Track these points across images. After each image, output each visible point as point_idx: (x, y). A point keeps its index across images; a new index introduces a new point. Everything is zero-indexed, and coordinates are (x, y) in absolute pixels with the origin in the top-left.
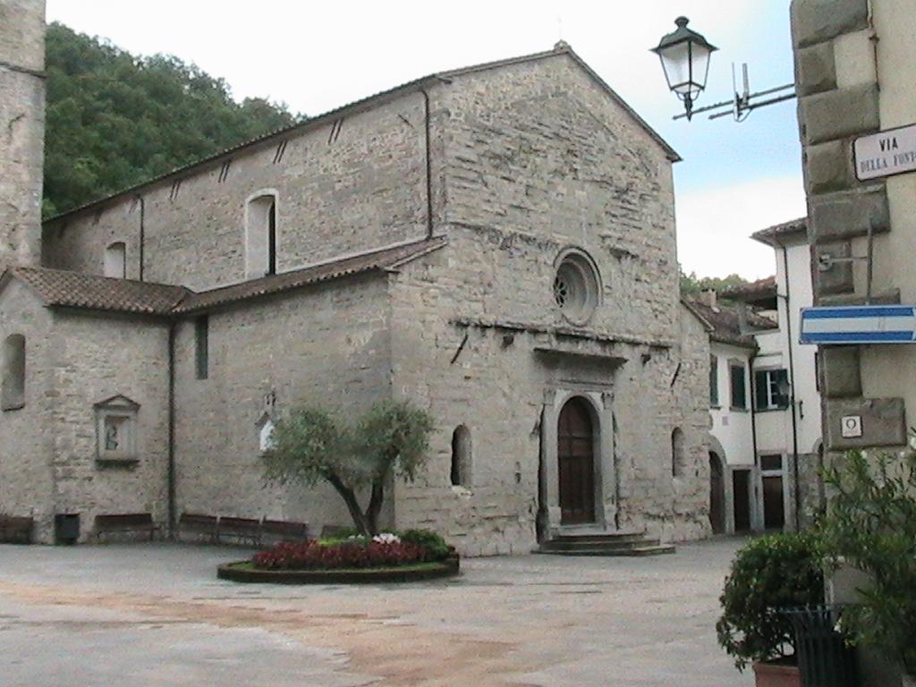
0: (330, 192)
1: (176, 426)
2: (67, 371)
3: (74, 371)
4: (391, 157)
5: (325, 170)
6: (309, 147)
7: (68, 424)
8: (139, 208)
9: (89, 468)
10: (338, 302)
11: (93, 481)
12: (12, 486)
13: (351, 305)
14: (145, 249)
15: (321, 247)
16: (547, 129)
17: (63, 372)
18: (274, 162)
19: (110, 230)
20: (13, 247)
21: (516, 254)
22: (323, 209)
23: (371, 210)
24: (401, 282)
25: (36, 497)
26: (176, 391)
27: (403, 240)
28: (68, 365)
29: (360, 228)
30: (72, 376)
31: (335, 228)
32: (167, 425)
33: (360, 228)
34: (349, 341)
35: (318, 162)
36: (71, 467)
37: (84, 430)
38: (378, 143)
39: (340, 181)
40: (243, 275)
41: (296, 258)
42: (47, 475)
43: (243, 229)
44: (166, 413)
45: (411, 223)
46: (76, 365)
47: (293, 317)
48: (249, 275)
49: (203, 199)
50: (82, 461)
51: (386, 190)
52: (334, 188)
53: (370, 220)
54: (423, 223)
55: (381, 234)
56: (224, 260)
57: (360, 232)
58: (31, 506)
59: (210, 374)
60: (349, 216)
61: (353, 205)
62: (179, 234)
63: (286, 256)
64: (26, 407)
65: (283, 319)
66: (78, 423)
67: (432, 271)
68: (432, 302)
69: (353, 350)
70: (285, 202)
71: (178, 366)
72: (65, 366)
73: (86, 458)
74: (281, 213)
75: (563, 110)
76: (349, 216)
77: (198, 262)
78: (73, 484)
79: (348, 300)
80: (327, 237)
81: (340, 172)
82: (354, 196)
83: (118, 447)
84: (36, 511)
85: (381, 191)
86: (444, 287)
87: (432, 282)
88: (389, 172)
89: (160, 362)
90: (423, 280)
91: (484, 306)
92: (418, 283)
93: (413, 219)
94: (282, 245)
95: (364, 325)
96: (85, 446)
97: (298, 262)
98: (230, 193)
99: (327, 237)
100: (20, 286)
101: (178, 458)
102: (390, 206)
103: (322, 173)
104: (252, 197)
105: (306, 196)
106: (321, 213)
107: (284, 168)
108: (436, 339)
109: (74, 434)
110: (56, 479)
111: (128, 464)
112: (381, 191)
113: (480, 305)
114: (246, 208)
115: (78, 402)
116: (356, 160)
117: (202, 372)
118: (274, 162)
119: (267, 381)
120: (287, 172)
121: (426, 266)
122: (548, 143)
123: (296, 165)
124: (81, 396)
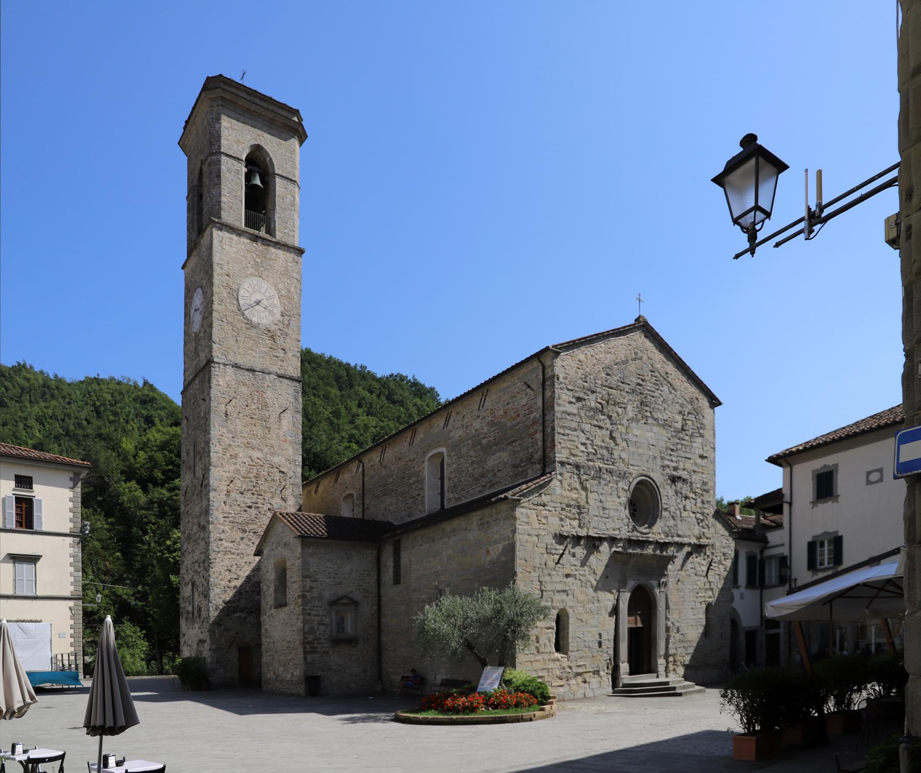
0: (479, 446)
1: (382, 616)
2: (311, 581)
3: (316, 581)
7: (312, 617)
8: (361, 469)
9: (326, 645)
10: (481, 525)
11: (330, 654)
12: (281, 658)
15: (474, 487)
16: (627, 386)
17: (309, 582)
18: (444, 428)
19: (345, 486)
20: (283, 499)
22: (473, 459)
23: (504, 455)
25: (294, 665)
26: (382, 593)
27: (526, 477)
28: (311, 577)
29: (499, 471)
30: (314, 585)
31: (482, 472)
32: (376, 615)
33: (499, 471)
34: (488, 552)
35: (471, 425)
36: (315, 645)
37: (323, 621)
39: (486, 437)
40: (425, 511)
41: (457, 496)
42: (301, 650)
43: (424, 479)
44: (375, 607)
45: (531, 463)
46: (317, 577)
47: (453, 538)
48: (428, 511)
49: (400, 459)
50: (322, 641)
52: (481, 444)
53: (505, 464)
54: (539, 463)
55: (511, 474)
57: (498, 474)
58: (291, 671)
59: (402, 581)
60: (492, 462)
61: (494, 454)
63: (451, 496)
64: (286, 608)
65: (446, 540)
66: (318, 615)
67: (545, 498)
68: (544, 521)
69: (491, 558)
70: (450, 456)
71: (382, 576)
72: (309, 577)
73: (325, 639)
74: (449, 465)
75: (639, 372)
76: (492, 462)
77: (397, 503)
78: (316, 656)
79: (487, 522)
80: (477, 480)
81: (485, 430)
82: (495, 448)
83: (345, 631)
84: (295, 673)
85: (513, 442)
86: (553, 509)
87: (544, 506)
88: (518, 427)
89: (371, 573)
90: (538, 505)
92: (534, 507)
93: (533, 460)
95: (497, 542)
96: (324, 631)
97: (459, 498)
98: (416, 453)
99: (477, 480)
100: (282, 524)
101: (384, 638)
103: (473, 432)
104: (430, 455)
105: (464, 451)
106: (473, 462)
109: (316, 623)
110: (305, 653)
111: (352, 641)
112: (513, 442)
114: (426, 464)
115: (319, 602)
116: (496, 421)
117: (397, 580)
118: (444, 428)
119: (436, 583)
120: (452, 434)
121: (540, 495)
122: (630, 397)
123: (457, 428)
124: (320, 598)
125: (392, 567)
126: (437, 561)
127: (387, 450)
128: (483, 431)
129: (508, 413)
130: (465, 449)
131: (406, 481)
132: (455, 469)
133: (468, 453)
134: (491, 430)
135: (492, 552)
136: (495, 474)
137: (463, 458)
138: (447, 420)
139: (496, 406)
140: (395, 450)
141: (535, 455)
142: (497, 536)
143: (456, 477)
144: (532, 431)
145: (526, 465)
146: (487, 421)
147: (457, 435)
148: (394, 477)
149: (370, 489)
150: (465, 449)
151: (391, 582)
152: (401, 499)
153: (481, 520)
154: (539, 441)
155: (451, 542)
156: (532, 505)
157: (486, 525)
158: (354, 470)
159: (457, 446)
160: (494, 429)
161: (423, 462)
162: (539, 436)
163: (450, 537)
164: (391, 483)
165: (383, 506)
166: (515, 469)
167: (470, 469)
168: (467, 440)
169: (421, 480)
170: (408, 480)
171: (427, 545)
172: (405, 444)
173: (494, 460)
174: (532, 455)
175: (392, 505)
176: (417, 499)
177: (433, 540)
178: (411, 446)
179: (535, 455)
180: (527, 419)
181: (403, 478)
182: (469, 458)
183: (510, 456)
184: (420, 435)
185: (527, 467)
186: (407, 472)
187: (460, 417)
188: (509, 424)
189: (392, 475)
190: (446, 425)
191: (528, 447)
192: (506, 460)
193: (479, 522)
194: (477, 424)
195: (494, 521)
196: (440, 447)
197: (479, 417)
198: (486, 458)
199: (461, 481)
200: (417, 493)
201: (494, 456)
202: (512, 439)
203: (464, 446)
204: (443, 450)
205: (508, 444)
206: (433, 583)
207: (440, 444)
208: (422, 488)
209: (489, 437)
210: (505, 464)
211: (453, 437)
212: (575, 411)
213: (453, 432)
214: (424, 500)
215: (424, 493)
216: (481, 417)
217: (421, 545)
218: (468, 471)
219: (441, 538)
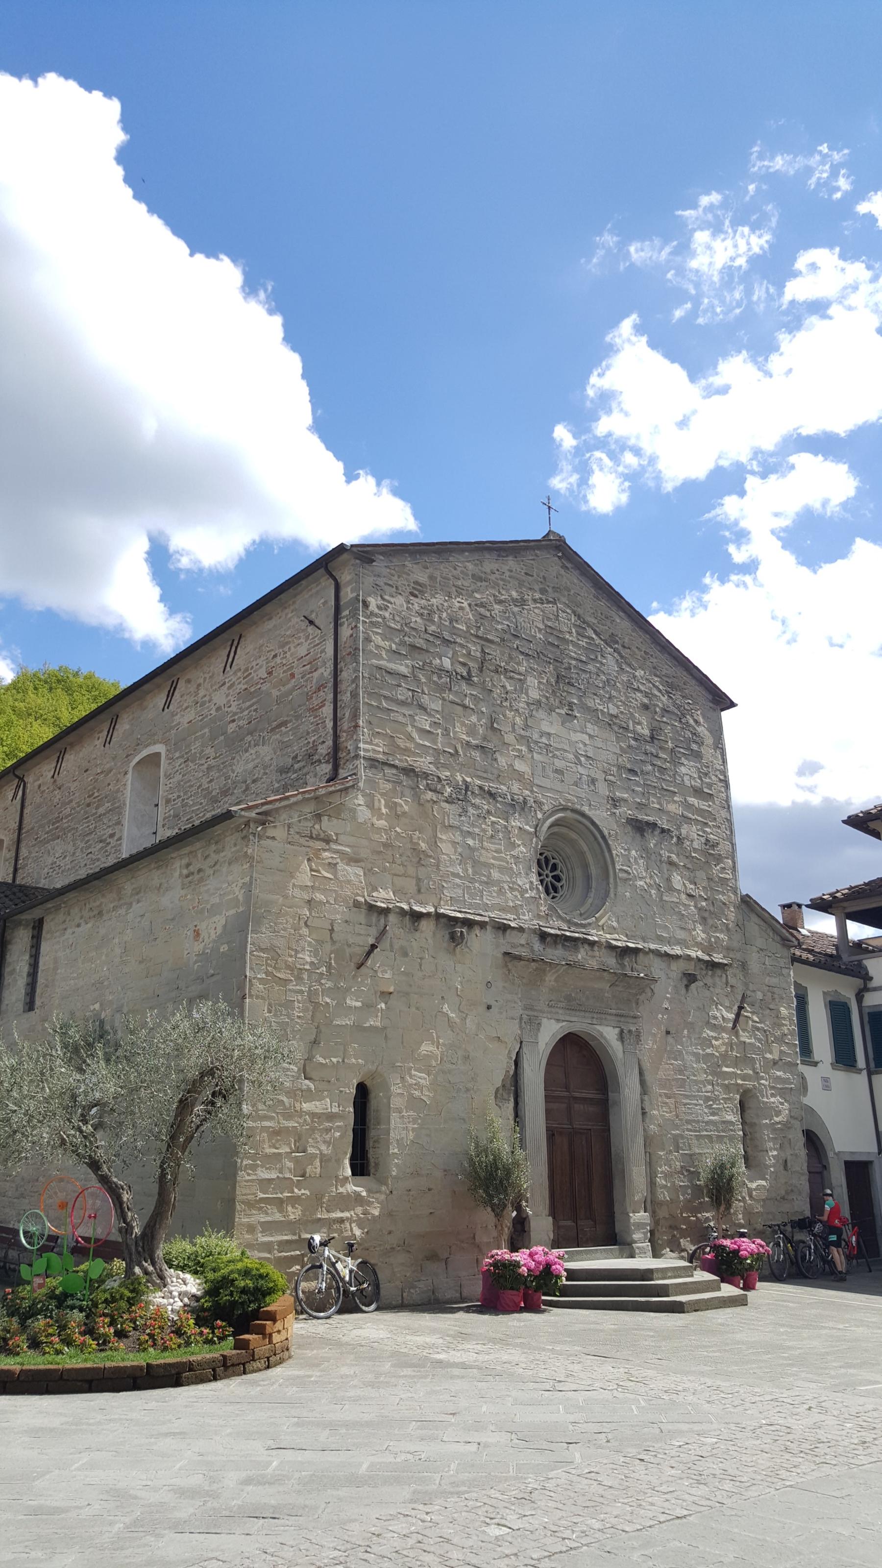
0: (222, 738)
4: (293, 676)
5: (219, 709)
6: (201, 681)
10: (187, 876)
13: (201, 880)
14: (23, 845)
18: (163, 710)
21: (471, 810)
22: (211, 762)
23: (266, 752)
24: (273, 838)
29: (254, 781)
33: (254, 781)
34: (197, 934)
38: (278, 660)
39: (233, 721)
43: (125, 804)
45: (312, 764)
51: (284, 724)
54: (327, 762)
55: (277, 785)
56: (102, 848)
60: (242, 766)
61: (247, 751)
62: (59, 820)
65: (122, 911)
76: (242, 766)
77: (74, 853)
81: (234, 709)
82: (249, 738)
85: (280, 726)
90: (311, 837)
91: (418, 885)
93: (316, 757)
94: (164, 820)
95: (214, 911)
102: (287, 745)
103: (213, 712)
104: (137, 759)
105: (195, 747)
106: (209, 768)
107: (173, 715)
108: (332, 930)
112: (280, 726)
113: (414, 882)
116: (252, 689)
118: (163, 710)
121: (318, 817)
123: (187, 708)
125: (25, 975)
126: (104, 958)
127: (67, 756)
128: (229, 709)
129: (275, 674)
130: (198, 744)
131: (94, 811)
132: (179, 783)
133: (203, 751)
134: (244, 706)
135: (204, 934)
136: (247, 789)
137: (192, 762)
138: (170, 695)
139: (254, 664)
140: (81, 755)
141: (320, 747)
142: (216, 900)
143: (179, 797)
144: (315, 702)
145: (304, 767)
146: (238, 691)
147: (186, 720)
148: (74, 804)
149: (32, 829)
150: (198, 744)
151: (20, 1006)
152: (83, 845)
153: (188, 865)
154: (327, 721)
155: (130, 917)
156: (297, 836)
157: (197, 877)
158: (10, 795)
159: (184, 739)
160: (248, 704)
161: (126, 773)
162: (327, 711)
163: (131, 904)
164: (66, 817)
165: (50, 860)
166: (284, 776)
167: (205, 781)
168: (202, 728)
169: (118, 807)
170: (97, 808)
171: (90, 925)
172: (97, 742)
173: (247, 762)
174: (315, 748)
175: (65, 857)
176: (109, 843)
177: (100, 914)
178: (107, 745)
179: (320, 747)
180: (307, 681)
181: (89, 805)
182: (203, 761)
183: (275, 753)
184: (124, 726)
185: (305, 770)
186: (96, 794)
187: (192, 688)
188: (275, 693)
189: (71, 801)
190: (167, 704)
191: (308, 733)
192: (267, 759)
193: (185, 872)
194: (219, 698)
195: (211, 867)
196: (155, 743)
197: (224, 684)
198: (233, 758)
199: (186, 805)
200: (111, 832)
201: (247, 754)
202: (279, 721)
203: (196, 739)
204: (160, 748)
205: (273, 730)
206: (92, 1008)
207: (156, 738)
208: (119, 823)
209: (240, 719)
210: (265, 768)
211: (179, 723)
212: (403, 670)
213: (179, 715)
214: (120, 845)
215: (121, 831)
216: (227, 685)
217: (79, 926)
218: (200, 786)
219: (115, 908)
